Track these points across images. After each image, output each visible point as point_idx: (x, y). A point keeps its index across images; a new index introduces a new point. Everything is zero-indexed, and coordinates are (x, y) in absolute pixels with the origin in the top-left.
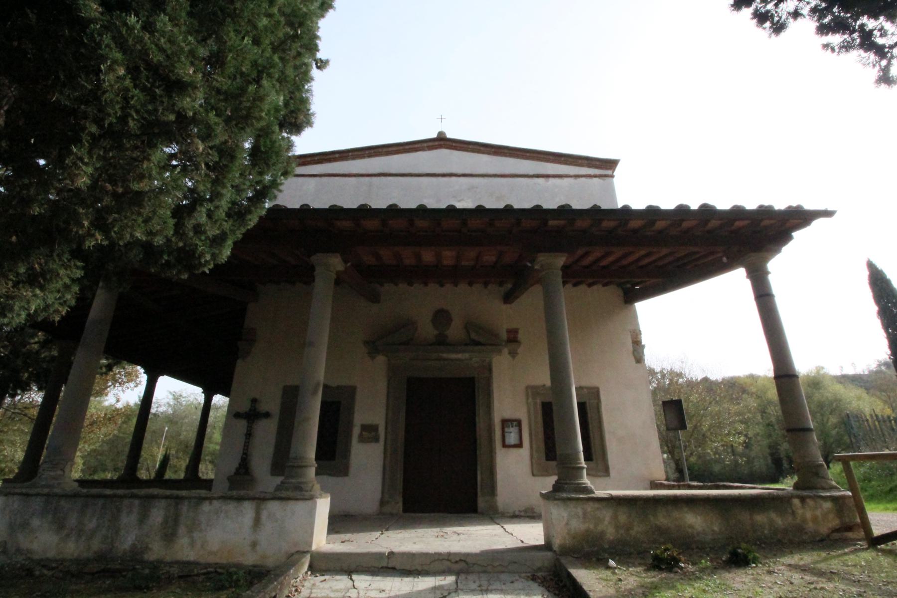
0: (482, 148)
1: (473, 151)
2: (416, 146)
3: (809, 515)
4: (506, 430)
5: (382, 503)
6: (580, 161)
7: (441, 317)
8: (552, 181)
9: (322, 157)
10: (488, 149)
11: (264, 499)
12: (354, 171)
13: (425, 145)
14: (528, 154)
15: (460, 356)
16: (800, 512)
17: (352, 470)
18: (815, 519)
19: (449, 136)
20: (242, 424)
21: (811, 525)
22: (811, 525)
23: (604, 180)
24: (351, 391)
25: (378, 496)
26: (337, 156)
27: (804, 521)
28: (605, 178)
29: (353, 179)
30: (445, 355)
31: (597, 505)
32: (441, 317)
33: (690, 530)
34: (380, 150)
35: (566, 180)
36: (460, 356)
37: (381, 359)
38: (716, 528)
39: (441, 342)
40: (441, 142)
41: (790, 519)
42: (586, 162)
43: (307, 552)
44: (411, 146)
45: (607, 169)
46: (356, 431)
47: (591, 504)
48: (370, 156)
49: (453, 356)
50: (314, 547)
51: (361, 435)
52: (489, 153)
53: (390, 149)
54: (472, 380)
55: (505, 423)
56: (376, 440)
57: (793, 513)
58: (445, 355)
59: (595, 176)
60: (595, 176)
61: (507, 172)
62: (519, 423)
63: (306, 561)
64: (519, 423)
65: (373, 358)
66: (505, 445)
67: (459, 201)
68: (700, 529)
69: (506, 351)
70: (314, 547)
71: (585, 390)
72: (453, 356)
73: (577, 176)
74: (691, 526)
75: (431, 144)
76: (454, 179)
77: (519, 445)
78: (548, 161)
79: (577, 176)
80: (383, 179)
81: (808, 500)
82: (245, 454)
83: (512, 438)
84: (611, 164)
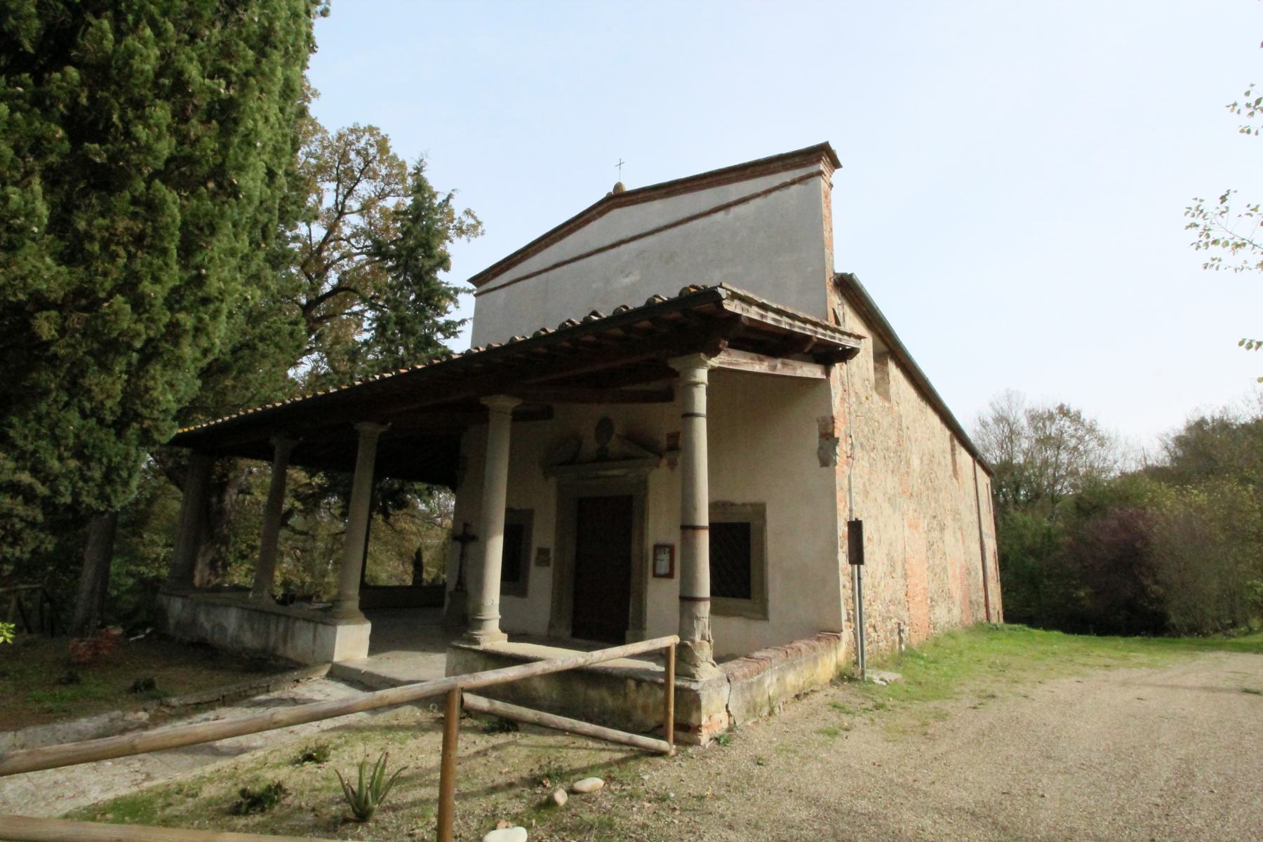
0: (652, 193)
1: (645, 200)
2: (586, 217)
3: (640, 701)
4: (659, 557)
5: (551, 626)
6: (772, 166)
7: (605, 426)
8: (735, 210)
9: (509, 262)
10: (659, 192)
11: (317, 623)
12: (535, 270)
13: (594, 212)
14: (704, 182)
15: (616, 472)
16: (632, 695)
17: (530, 593)
18: (645, 708)
19: (629, 187)
20: (458, 544)
21: (640, 712)
22: (640, 712)
23: (806, 184)
24: (529, 514)
25: (548, 619)
26: (519, 256)
27: (634, 707)
28: (809, 180)
29: (533, 280)
30: (601, 473)
31: (475, 656)
32: (605, 426)
33: (534, 693)
34: (553, 236)
35: (753, 204)
36: (616, 472)
37: (552, 480)
38: (554, 696)
39: (603, 457)
40: (619, 199)
41: (621, 700)
42: (781, 164)
43: (328, 662)
44: (581, 220)
45: (812, 163)
46: (533, 555)
47: (471, 654)
48: (547, 246)
49: (610, 473)
50: (337, 658)
51: (537, 558)
52: (661, 197)
53: (562, 231)
54: (630, 498)
55: (658, 548)
56: (548, 565)
57: (625, 695)
58: (601, 473)
59: (793, 183)
60: (793, 183)
61: (680, 217)
62: (671, 549)
63: (328, 667)
64: (671, 549)
65: (546, 478)
66: (655, 575)
67: (627, 276)
68: (541, 694)
69: (664, 461)
70: (337, 658)
71: (749, 507)
72: (610, 473)
73: (767, 192)
74: (535, 689)
75: (600, 209)
76: (623, 247)
77: (670, 575)
78: (729, 181)
79: (767, 192)
80: (558, 271)
81: (644, 684)
82: (460, 572)
83: (663, 567)
84: (821, 154)
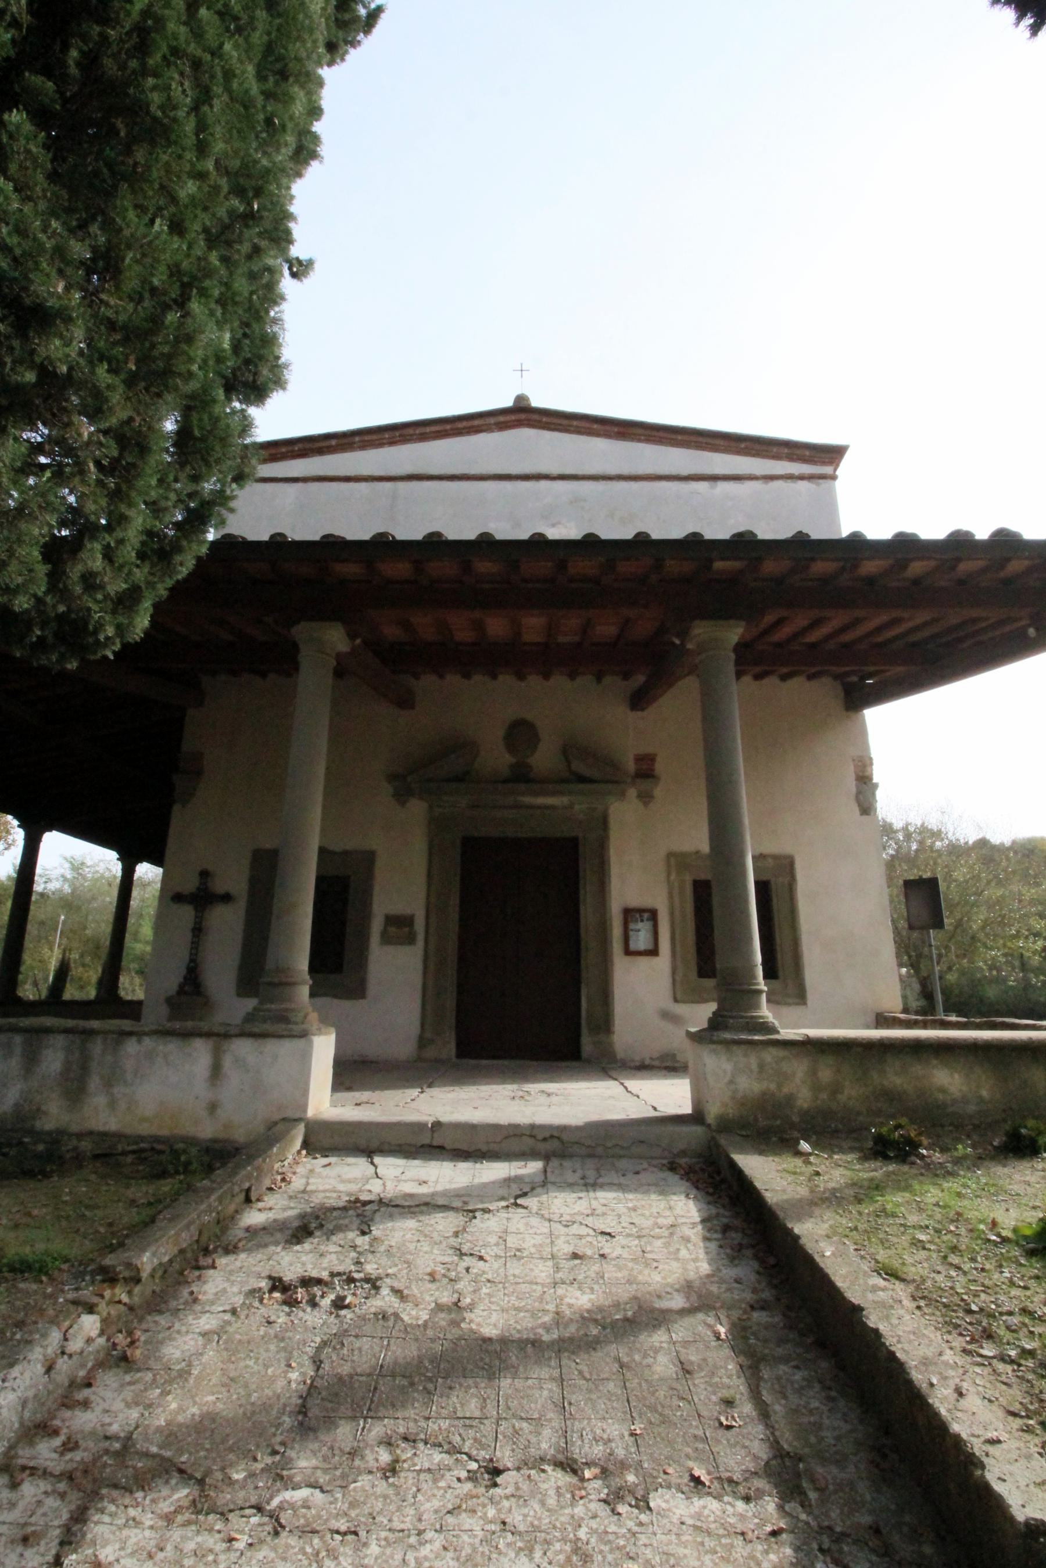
1: (579, 431)
2: (476, 422)
4: (632, 926)
5: (423, 1042)
8: (723, 487)
10: (608, 428)
11: (227, 1036)
13: (492, 420)
14: (680, 437)
19: (535, 403)
20: (186, 913)
23: (818, 485)
25: (415, 1029)
26: (333, 442)
28: (821, 481)
29: (362, 486)
30: (528, 800)
31: (781, 1053)
33: (941, 1096)
34: (410, 431)
37: (417, 808)
38: (985, 1093)
42: (786, 451)
44: (465, 424)
45: (824, 463)
46: (377, 926)
48: (392, 443)
49: (540, 801)
50: (310, 1113)
52: (608, 435)
54: (574, 842)
55: (629, 914)
56: (411, 940)
58: (528, 800)
59: (801, 478)
60: (801, 478)
61: (641, 470)
64: (653, 915)
66: (628, 952)
67: (553, 525)
68: (957, 1094)
69: (632, 792)
70: (310, 1113)
71: (770, 860)
72: (540, 801)
74: (943, 1090)
75: (501, 419)
76: (543, 484)
77: (654, 952)
78: (715, 449)
82: (192, 961)
83: (641, 939)
84: (832, 454)
